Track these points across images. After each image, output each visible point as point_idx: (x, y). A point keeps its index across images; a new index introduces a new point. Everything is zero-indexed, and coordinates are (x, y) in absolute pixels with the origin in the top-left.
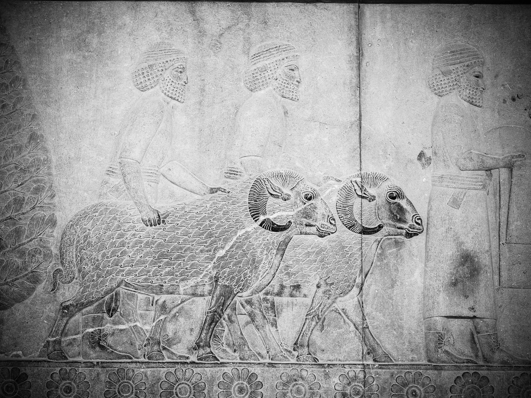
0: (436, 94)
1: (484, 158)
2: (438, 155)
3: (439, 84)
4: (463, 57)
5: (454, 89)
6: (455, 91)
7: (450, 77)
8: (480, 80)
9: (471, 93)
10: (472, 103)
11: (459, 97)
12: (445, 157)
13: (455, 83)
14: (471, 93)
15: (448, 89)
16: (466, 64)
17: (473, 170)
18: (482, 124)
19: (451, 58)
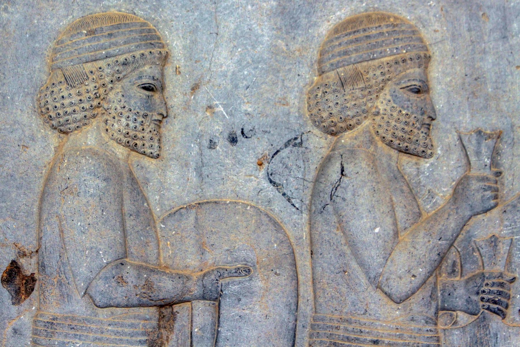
0: (54, 128)
1: (154, 278)
2: (48, 270)
3: (58, 105)
4: (116, 44)
5: (94, 116)
6: (94, 122)
7: (83, 89)
8: (157, 96)
9: (132, 125)
10: (134, 148)
11: (103, 134)
12: (63, 276)
13: (95, 103)
14: (132, 125)
15: (79, 116)
16: (121, 59)
17: (127, 306)
18: (157, 197)
19: (87, 45)
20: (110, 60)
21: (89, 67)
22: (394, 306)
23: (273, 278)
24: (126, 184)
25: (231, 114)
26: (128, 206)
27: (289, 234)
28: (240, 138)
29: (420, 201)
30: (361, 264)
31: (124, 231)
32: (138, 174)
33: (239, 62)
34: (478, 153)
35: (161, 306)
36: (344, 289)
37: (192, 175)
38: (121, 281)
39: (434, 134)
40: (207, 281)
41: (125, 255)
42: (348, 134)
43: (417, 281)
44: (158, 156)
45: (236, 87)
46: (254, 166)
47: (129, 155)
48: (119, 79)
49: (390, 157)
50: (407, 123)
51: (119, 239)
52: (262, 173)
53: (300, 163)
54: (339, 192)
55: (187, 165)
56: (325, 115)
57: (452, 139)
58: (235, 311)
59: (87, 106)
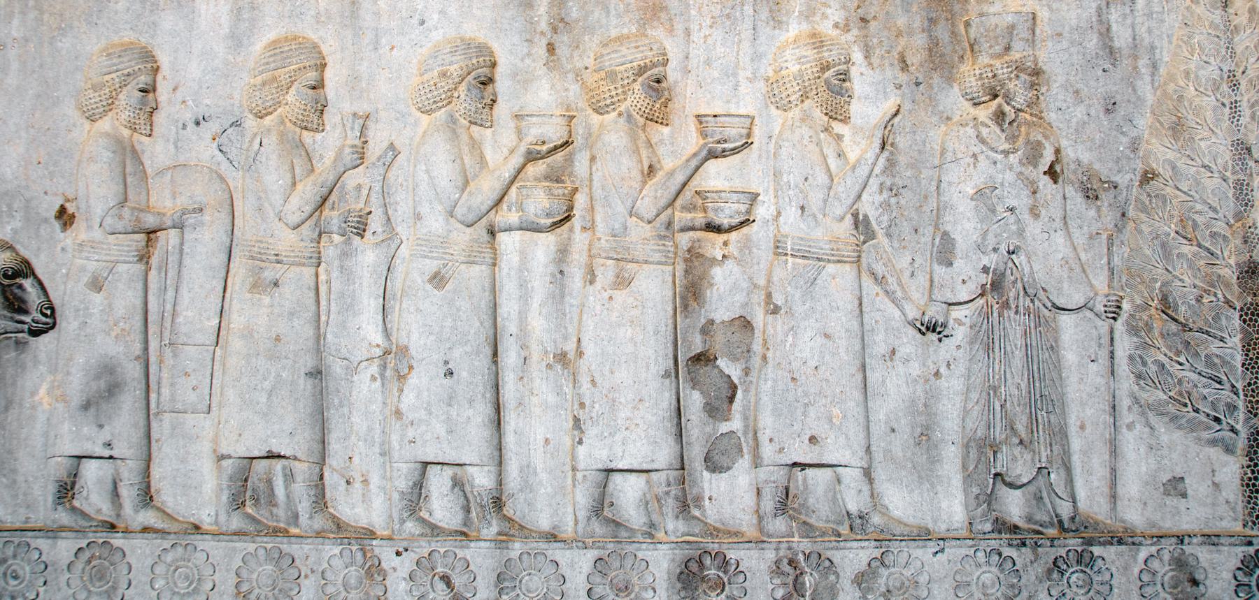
5: (111, 110)
6: (110, 114)
8: (151, 95)
9: (132, 115)
13: (110, 101)
14: (132, 115)
16: (126, 72)
20: (118, 73)
21: (107, 78)
22: (291, 231)
23: (217, 214)
24: (129, 154)
25: (197, 106)
26: (129, 169)
27: (231, 184)
28: (202, 122)
29: (314, 162)
30: (271, 205)
31: (125, 185)
32: (138, 147)
33: (204, 70)
34: (352, 129)
35: (149, 233)
36: (259, 221)
37: (172, 147)
38: (120, 217)
39: (325, 116)
40: (175, 217)
41: (126, 200)
42: (269, 118)
43: (305, 215)
44: (150, 135)
45: (201, 87)
46: (211, 140)
47: (132, 135)
48: (125, 85)
49: (295, 132)
50: (305, 110)
51: (122, 191)
52: (215, 144)
53: (239, 138)
54: (258, 157)
55: (168, 140)
56: (254, 105)
57: (337, 119)
58: (193, 236)
59: (105, 103)
